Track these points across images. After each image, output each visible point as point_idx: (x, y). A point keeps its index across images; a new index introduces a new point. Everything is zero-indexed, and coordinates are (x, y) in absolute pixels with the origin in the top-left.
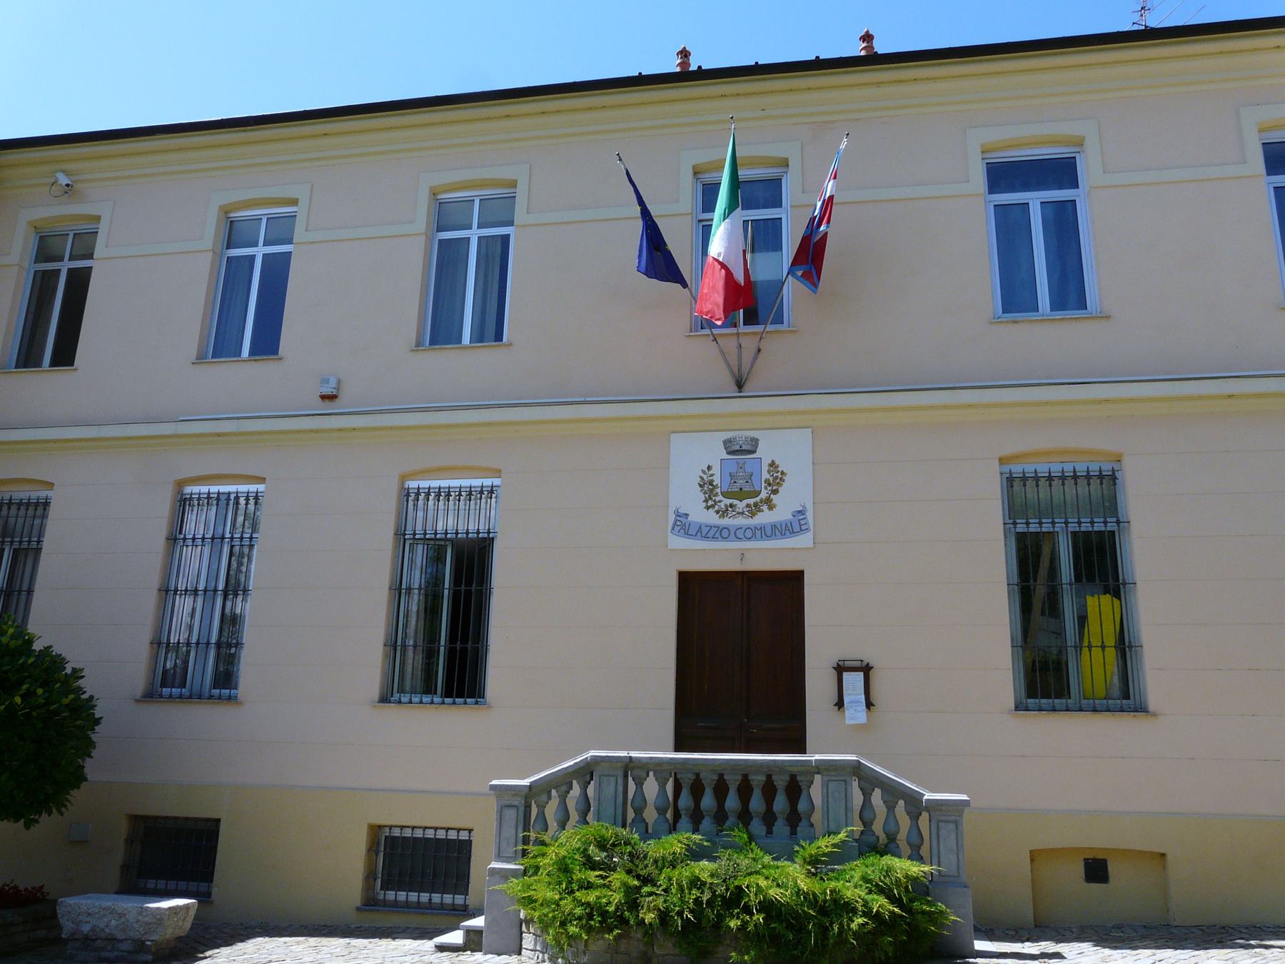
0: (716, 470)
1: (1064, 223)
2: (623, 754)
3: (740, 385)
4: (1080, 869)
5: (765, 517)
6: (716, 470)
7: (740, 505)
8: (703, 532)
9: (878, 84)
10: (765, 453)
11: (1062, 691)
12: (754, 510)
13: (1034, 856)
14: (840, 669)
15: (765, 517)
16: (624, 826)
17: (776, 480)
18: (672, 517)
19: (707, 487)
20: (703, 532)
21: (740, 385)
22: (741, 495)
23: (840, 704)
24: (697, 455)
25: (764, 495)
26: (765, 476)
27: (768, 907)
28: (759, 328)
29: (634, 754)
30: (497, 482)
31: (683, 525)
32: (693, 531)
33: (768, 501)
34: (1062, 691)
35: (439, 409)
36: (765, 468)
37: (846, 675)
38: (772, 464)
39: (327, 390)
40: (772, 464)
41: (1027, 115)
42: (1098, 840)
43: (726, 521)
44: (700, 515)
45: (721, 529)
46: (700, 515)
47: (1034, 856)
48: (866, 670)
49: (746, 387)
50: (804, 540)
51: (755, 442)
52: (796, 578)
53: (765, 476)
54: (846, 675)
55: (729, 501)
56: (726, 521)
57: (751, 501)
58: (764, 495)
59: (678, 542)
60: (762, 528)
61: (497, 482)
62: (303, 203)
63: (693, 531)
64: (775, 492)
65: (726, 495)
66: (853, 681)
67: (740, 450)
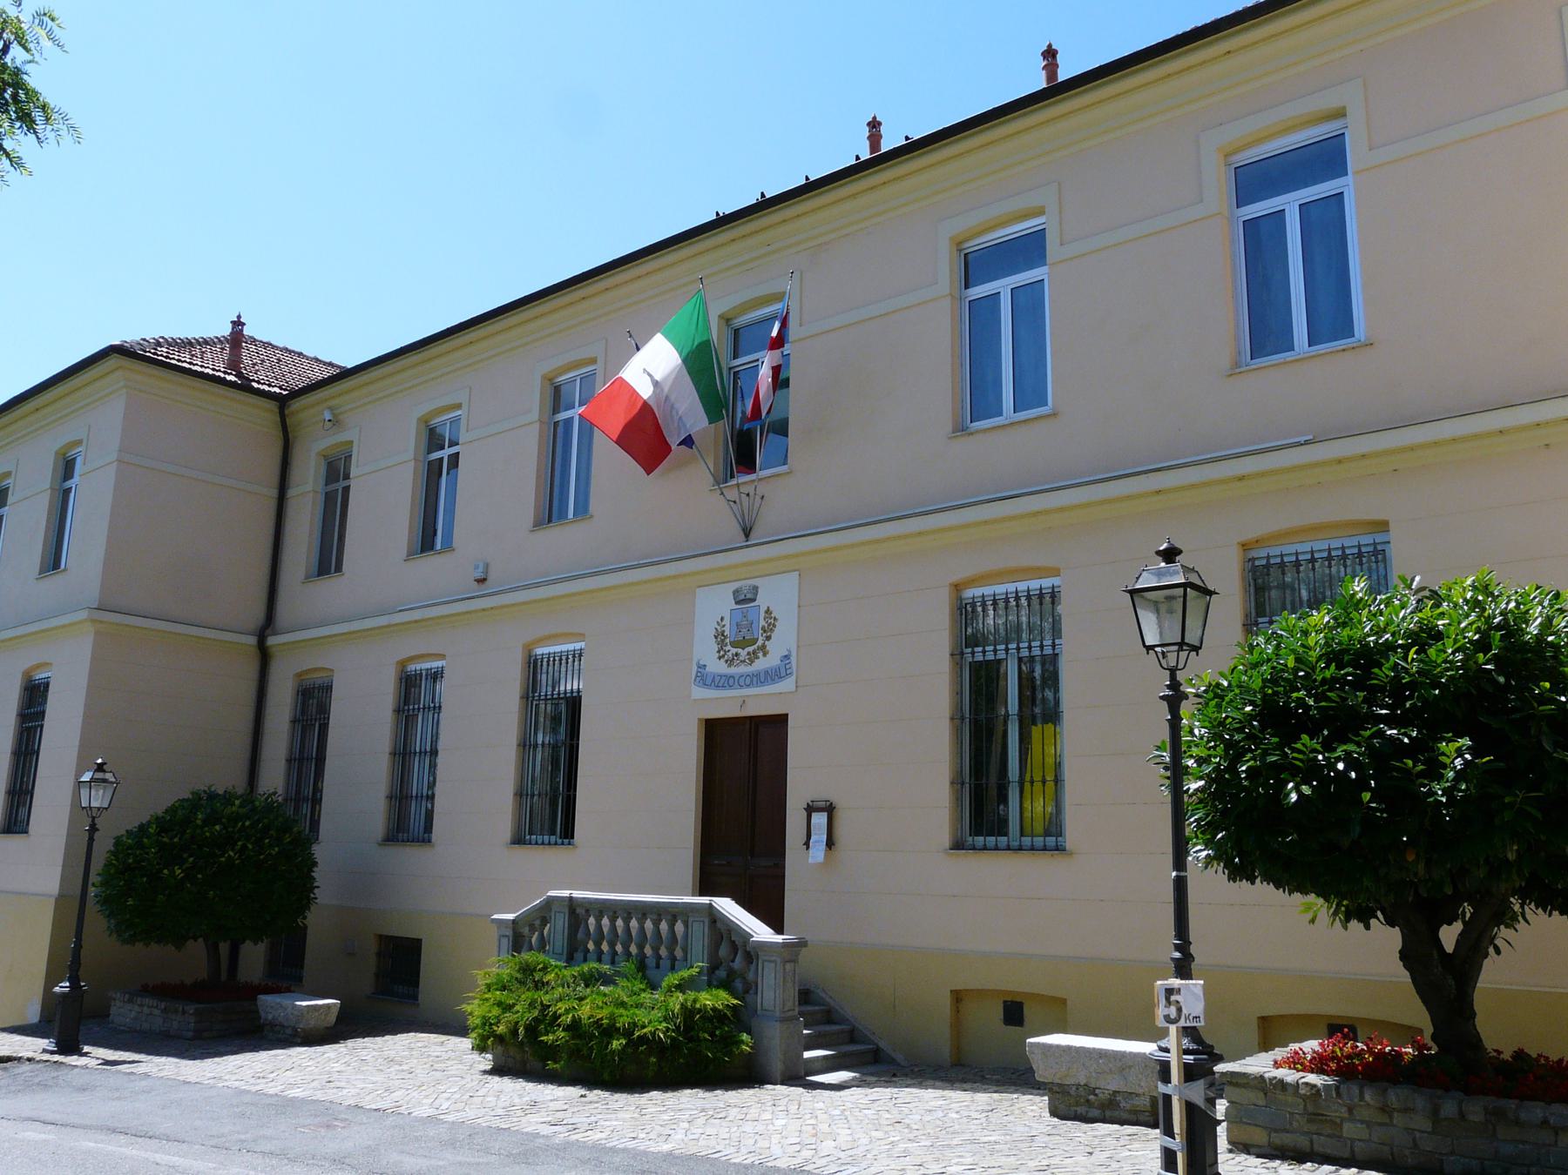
0: (727, 621)
1: (1326, 225)
2: (565, 893)
3: (747, 533)
4: (999, 1012)
5: (761, 664)
6: (727, 621)
7: (743, 653)
8: (726, 682)
9: (854, 196)
10: (763, 601)
11: (1000, 828)
12: (753, 657)
13: (958, 997)
14: (810, 809)
15: (761, 664)
16: (599, 960)
17: (768, 631)
18: (695, 668)
19: (720, 636)
20: (726, 682)
21: (747, 533)
22: (742, 643)
23: (807, 844)
24: (715, 606)
25: (760, 643)
26: (762, 623)
27: (575, 1027)
28: (752, 477)
29: (577, 894)
30: (1056, 581)
31: (704, 678)
32: (709, 681)
33: (763, 647)
34: (1000, 828)
35: (555, 582)
36: (762, 614)
37: (814, 815)
38: (768, 611)
39: (479, 575)
40: (768, 611)
41: (979, 196)
42: (1015, 983)
43: (733, 670)
44: (717, 667)
45: (729, 677)
46: (717, 667)
47: (958, 997)
48: (830, 809)
49: (752, 535)
50: (787, 685)
51: (756, 588)
52: (782, 720)
53: (762, 623)
54: (814, 815)
55: (734, 651)
56: (733, 670)
57: (751, 649)
58: (760, 643)
59: (699, 693)
60: (757, 675)
61: (1056, 581)
62: (465, 406)
63: (709, 681)
64: (768, 638)
65: (734, 645)
66: (820, 819)
67: (745, 598)
